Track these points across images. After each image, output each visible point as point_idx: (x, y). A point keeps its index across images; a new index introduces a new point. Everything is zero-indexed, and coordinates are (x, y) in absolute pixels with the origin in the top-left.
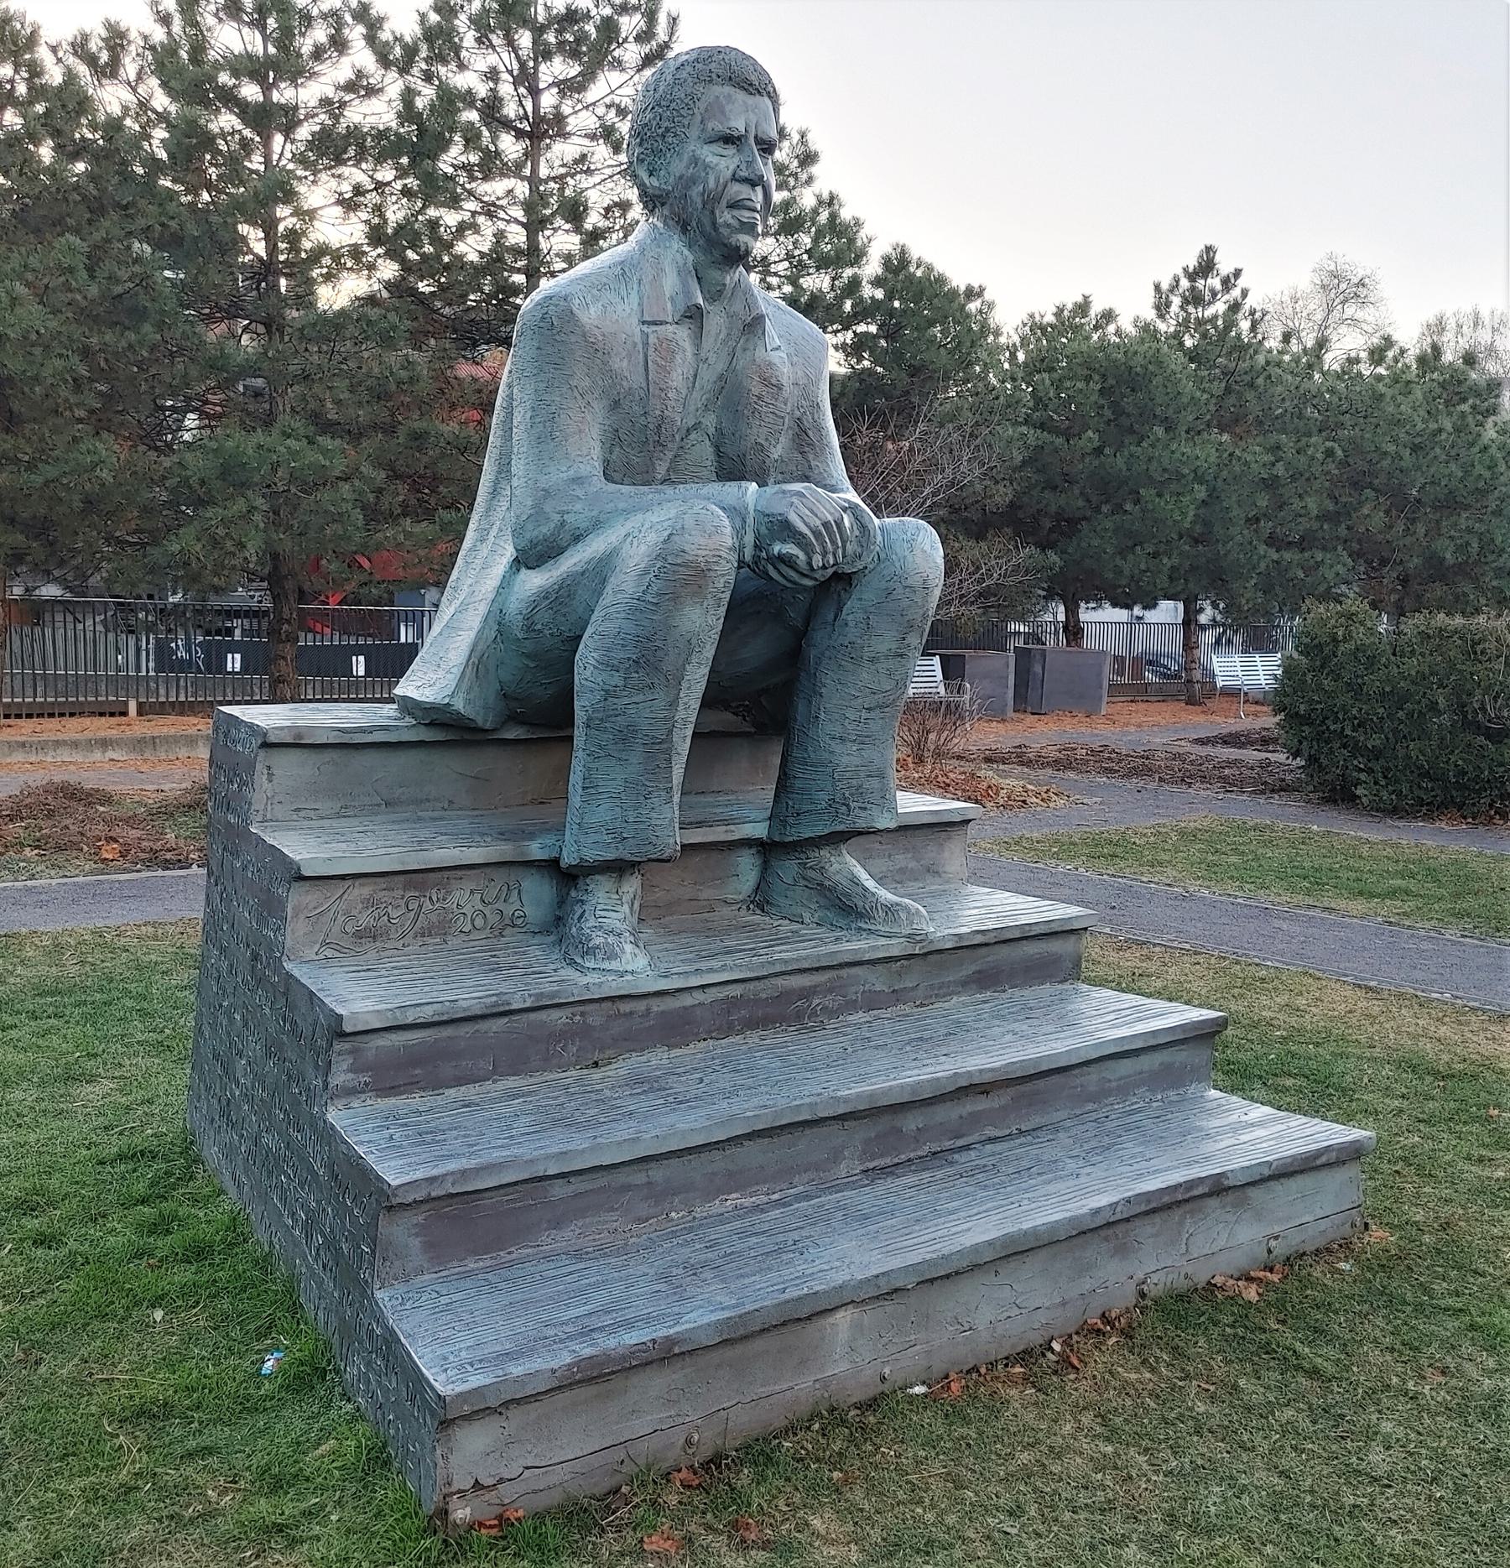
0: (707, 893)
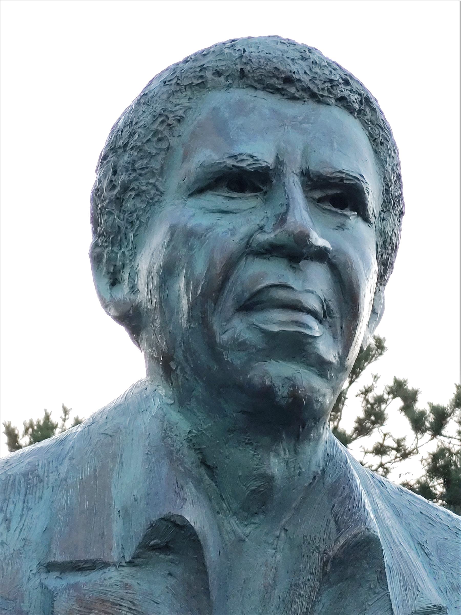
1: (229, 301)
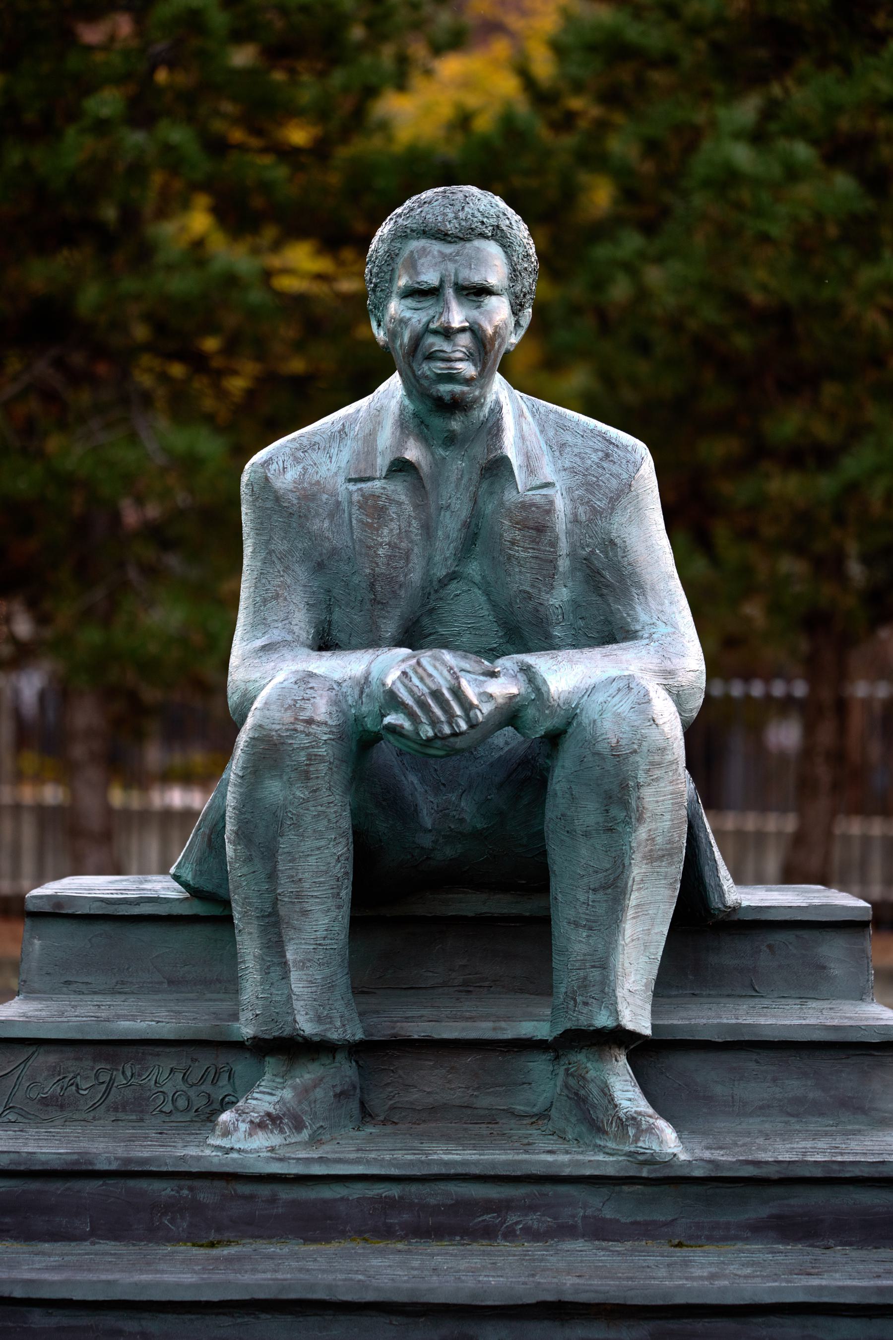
0: (485, 1101)
1: (419, 355)
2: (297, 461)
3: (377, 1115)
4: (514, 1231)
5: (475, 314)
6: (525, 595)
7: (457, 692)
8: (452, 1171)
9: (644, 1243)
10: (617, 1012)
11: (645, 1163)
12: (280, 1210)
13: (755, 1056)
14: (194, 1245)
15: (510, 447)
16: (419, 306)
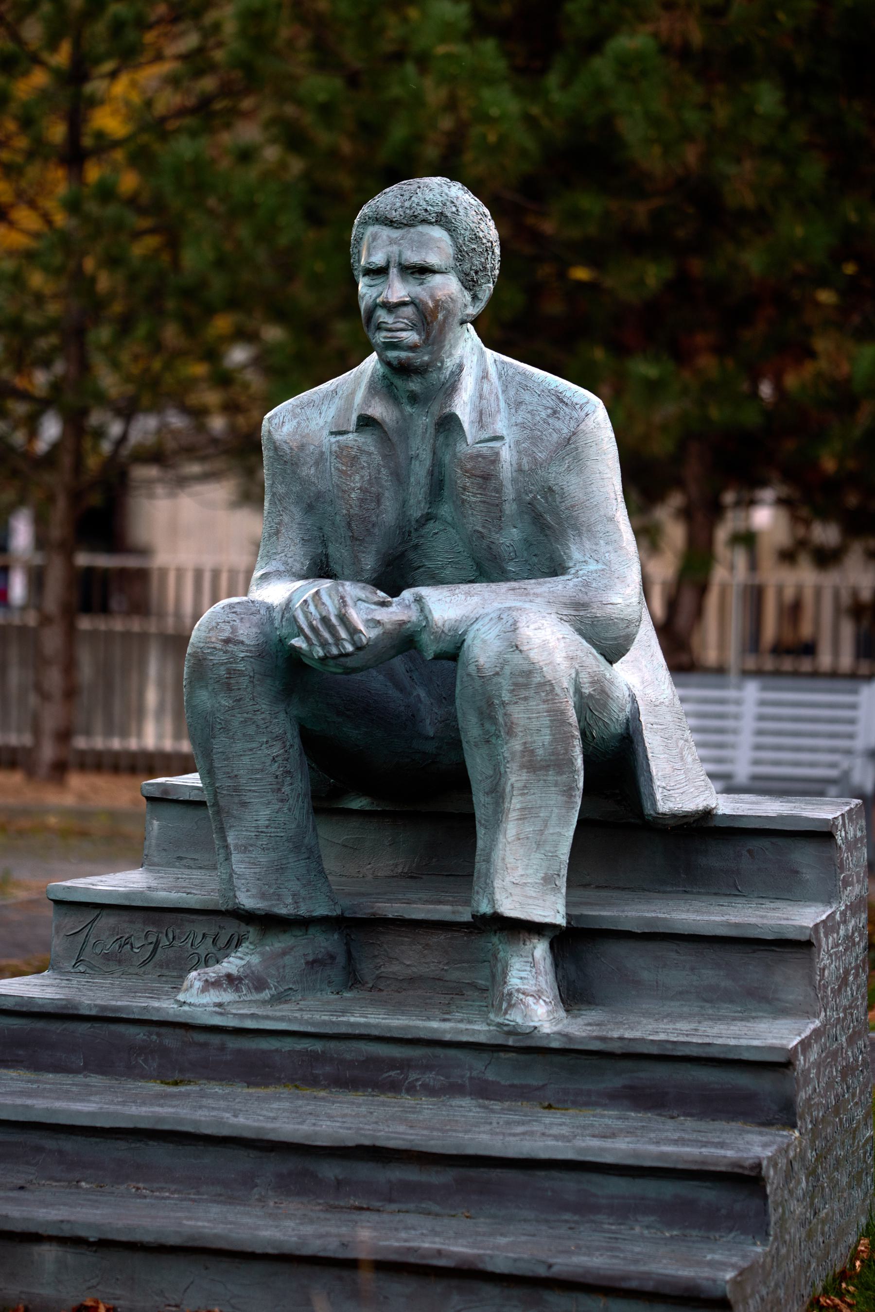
2: (295, 416)
3: (367, 983)
4: (415, 1086)
5: (418, 289)
6: (479, 535)
7: (343, 619)
8: (357, 1032)
9: (519, 1104)
10: (494, 901)
11: (509, 1033)
12: (229, 1057)
13: (675, 947)
14: (162, 1083)
15: (463, 406)
16: (373, 283)
